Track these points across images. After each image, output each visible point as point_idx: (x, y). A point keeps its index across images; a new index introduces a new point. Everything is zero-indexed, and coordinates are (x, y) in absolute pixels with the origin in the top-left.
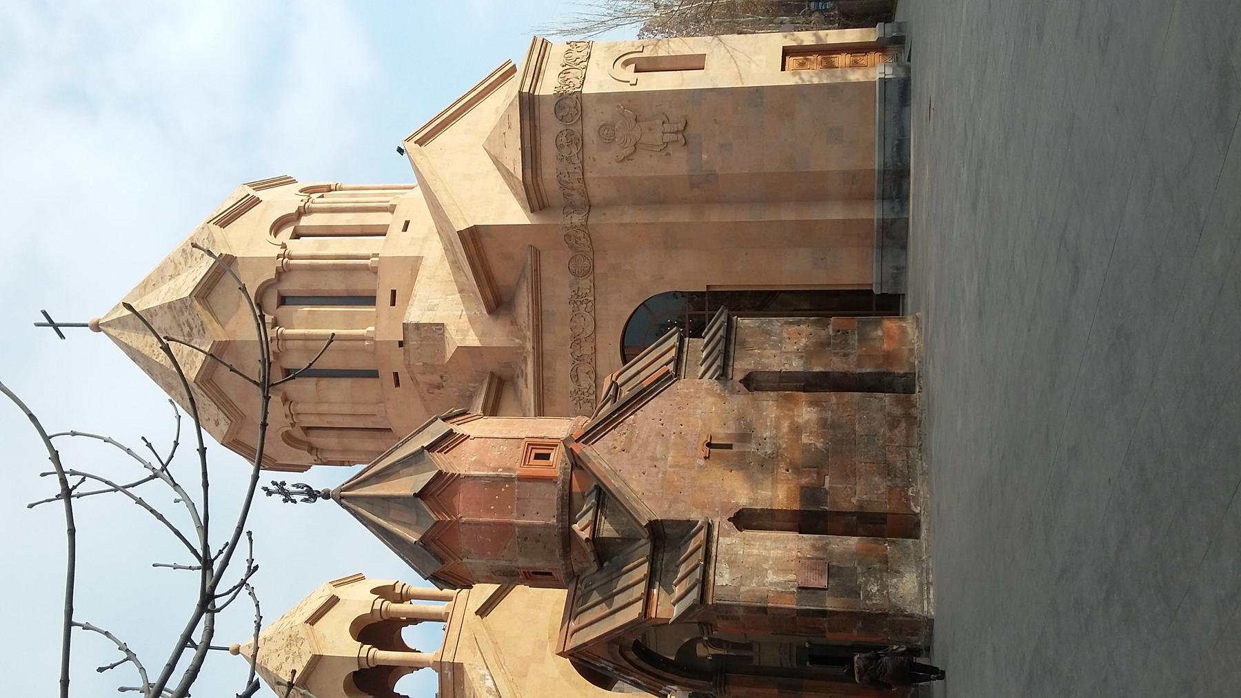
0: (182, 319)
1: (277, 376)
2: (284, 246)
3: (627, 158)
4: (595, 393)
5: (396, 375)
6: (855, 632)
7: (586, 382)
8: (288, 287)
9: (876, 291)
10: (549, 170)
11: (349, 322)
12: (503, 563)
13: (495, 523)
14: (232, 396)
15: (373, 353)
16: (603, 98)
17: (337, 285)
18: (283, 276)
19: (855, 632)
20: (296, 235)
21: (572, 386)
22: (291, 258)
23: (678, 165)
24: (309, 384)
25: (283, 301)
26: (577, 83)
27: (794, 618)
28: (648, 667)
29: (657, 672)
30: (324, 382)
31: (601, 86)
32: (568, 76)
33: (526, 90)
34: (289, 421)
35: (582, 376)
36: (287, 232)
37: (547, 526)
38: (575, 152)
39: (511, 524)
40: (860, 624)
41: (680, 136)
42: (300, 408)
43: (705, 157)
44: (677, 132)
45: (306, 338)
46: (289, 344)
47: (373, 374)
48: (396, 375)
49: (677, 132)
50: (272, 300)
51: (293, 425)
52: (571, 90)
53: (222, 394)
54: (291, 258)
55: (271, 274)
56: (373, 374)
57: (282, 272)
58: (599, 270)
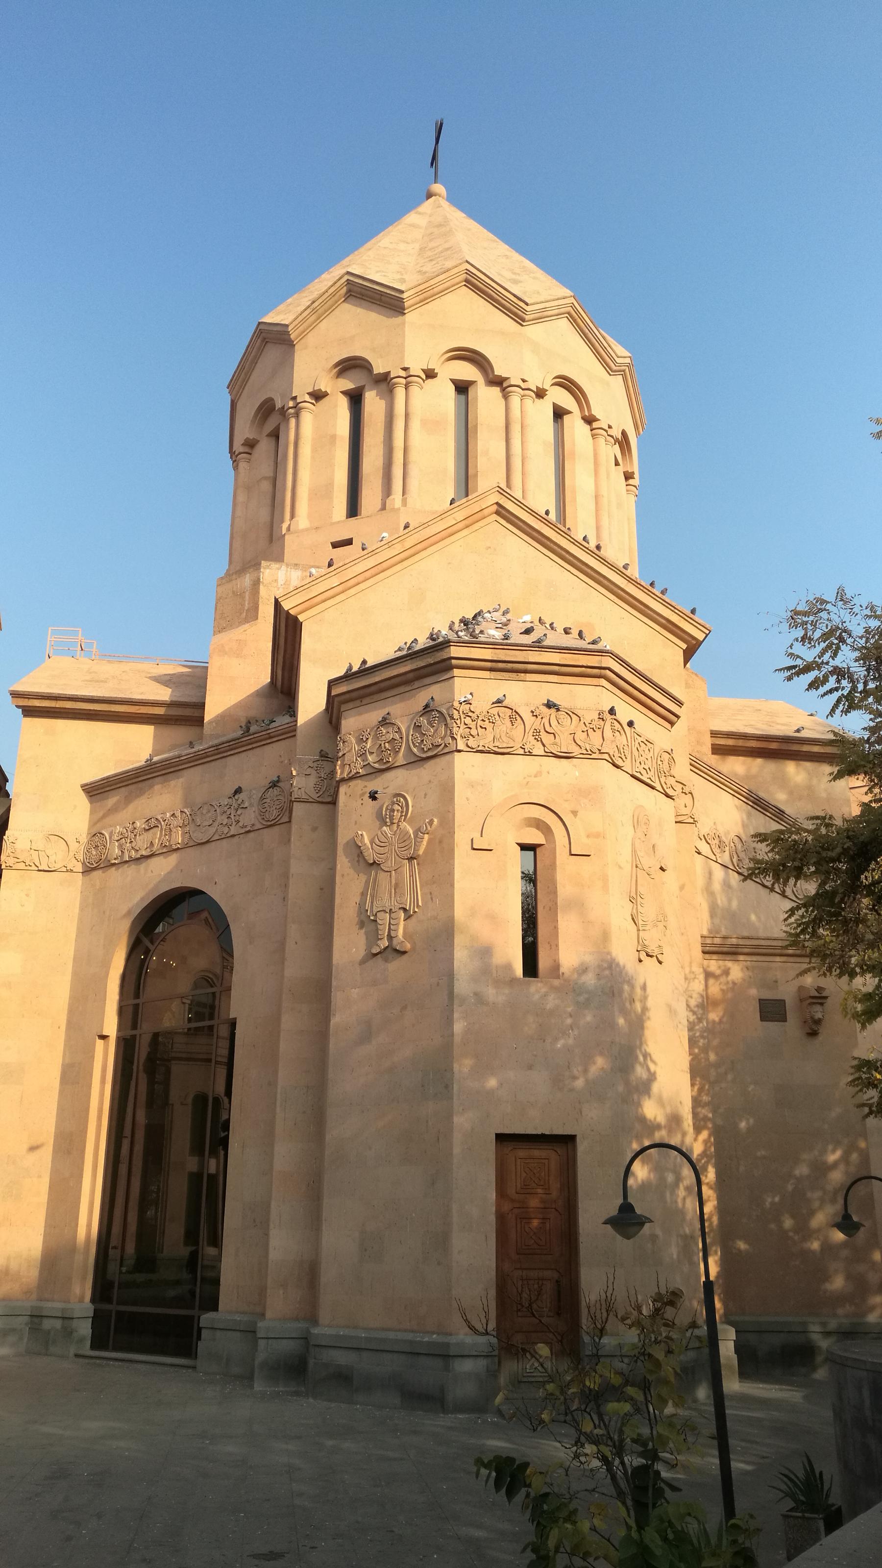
2: (430, 374)
3: (361, 854)
7: (142, 843)
9: (206, 1318)
11: (323, 493)
16: (447, 791)
18: (383, 386)
20: (462, 388)
22: (407, 387)
23: (348, 945)
25: (355, 399)
26: (486, 740)
31: (472, 785)
32: (504, 726)
33: (455, 651)
36: (467, 371)
38: (371, 759)
41: (385, 943)
43: (355, 993)
44: (390, 938)
49: (390, 938)
52: (459, 731)
53: (255, 362)
54: (407, 387)
55: (379, 368)
57: (384, 381)
58: (270, 836)
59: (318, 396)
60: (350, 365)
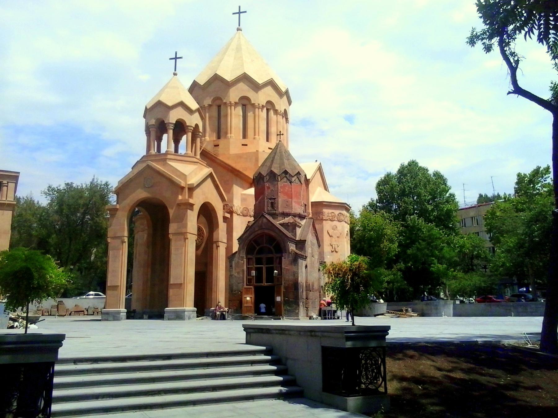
1: (245, 102)
5: (247, 145)
8: (271, 112)
10: (326, 211)
15: (254, 138)
39: (292, 198)
46: (257, 109)
48: (247, 145)
51: (225, 103)
56: (245, 136)
60: (269, 102)
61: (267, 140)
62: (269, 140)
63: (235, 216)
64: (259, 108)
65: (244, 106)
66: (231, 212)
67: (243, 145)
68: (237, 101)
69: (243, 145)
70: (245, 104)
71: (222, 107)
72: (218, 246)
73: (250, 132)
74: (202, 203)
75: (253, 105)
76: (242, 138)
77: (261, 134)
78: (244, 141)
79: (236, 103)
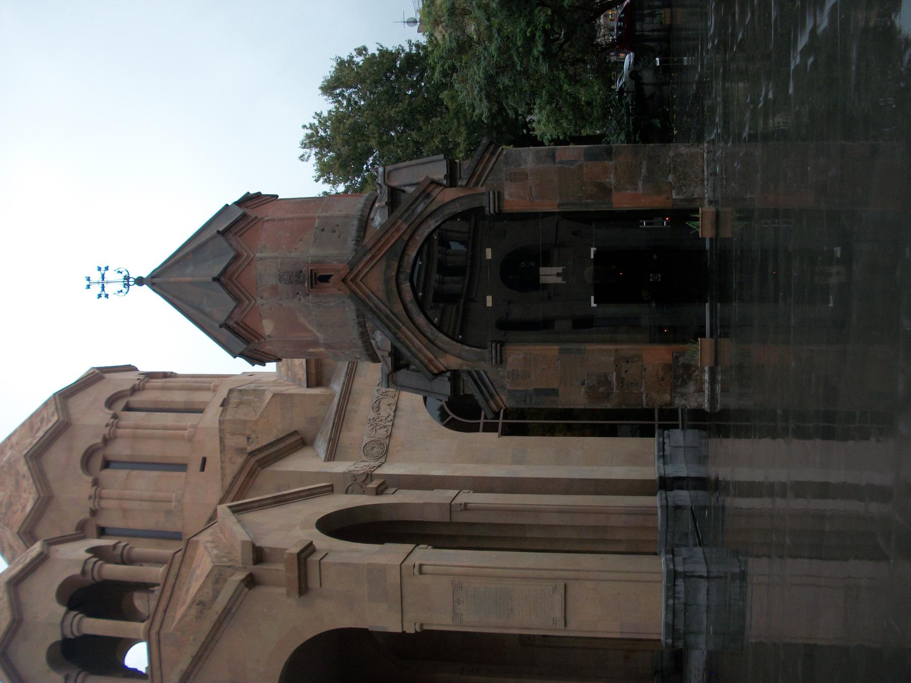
0: (39, 419)
1: (97, 461)
4: (393, 421)
6: (640, 184)
8: (136, 399)
12: (294, 255)
13: (298, 218)
14: (51, 474)
15: (190, 439)
17: (179, 397)
19: (640, 184)
21: (372, 415)
24: (122, 474)
25: (128, 408)
27: (581, 167)
28: (421, 320)
29: (430, 330)
30: (135, 473)
34: (90, 504)
35: (383, 406)
37: (346, 217)
39: (314, 218)
40: (644, 170)
42: (105, 492)
45: (137, 427)
47: (182, 467)
50: (121, 404)
51: (94, 513)
56: (182, 467)
59: (115, 417)
61: (201, 411)
62: (201, 407)
63: (378, 472)
64: (118, 427)
65: (107, 464)
66: (369, 476)
67: (203, 469)
68: (90, 479)
69: (203, 469)
70: (98, 459)
71: (103, 522)
72: (465, 507)
73: (175, 452)
74: (317, 531)
75: (106, 441)
76: (183, 474)
77: (180, 424)
78: (195, 466)
79: (96, 483)
